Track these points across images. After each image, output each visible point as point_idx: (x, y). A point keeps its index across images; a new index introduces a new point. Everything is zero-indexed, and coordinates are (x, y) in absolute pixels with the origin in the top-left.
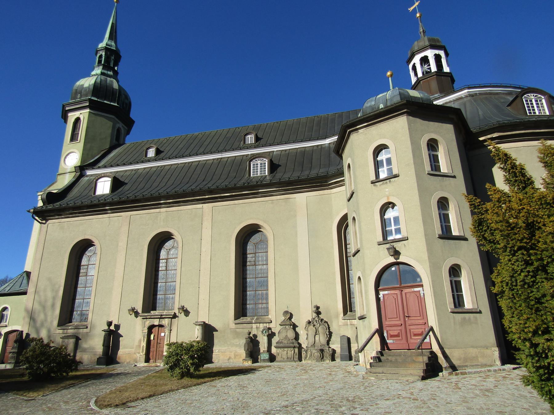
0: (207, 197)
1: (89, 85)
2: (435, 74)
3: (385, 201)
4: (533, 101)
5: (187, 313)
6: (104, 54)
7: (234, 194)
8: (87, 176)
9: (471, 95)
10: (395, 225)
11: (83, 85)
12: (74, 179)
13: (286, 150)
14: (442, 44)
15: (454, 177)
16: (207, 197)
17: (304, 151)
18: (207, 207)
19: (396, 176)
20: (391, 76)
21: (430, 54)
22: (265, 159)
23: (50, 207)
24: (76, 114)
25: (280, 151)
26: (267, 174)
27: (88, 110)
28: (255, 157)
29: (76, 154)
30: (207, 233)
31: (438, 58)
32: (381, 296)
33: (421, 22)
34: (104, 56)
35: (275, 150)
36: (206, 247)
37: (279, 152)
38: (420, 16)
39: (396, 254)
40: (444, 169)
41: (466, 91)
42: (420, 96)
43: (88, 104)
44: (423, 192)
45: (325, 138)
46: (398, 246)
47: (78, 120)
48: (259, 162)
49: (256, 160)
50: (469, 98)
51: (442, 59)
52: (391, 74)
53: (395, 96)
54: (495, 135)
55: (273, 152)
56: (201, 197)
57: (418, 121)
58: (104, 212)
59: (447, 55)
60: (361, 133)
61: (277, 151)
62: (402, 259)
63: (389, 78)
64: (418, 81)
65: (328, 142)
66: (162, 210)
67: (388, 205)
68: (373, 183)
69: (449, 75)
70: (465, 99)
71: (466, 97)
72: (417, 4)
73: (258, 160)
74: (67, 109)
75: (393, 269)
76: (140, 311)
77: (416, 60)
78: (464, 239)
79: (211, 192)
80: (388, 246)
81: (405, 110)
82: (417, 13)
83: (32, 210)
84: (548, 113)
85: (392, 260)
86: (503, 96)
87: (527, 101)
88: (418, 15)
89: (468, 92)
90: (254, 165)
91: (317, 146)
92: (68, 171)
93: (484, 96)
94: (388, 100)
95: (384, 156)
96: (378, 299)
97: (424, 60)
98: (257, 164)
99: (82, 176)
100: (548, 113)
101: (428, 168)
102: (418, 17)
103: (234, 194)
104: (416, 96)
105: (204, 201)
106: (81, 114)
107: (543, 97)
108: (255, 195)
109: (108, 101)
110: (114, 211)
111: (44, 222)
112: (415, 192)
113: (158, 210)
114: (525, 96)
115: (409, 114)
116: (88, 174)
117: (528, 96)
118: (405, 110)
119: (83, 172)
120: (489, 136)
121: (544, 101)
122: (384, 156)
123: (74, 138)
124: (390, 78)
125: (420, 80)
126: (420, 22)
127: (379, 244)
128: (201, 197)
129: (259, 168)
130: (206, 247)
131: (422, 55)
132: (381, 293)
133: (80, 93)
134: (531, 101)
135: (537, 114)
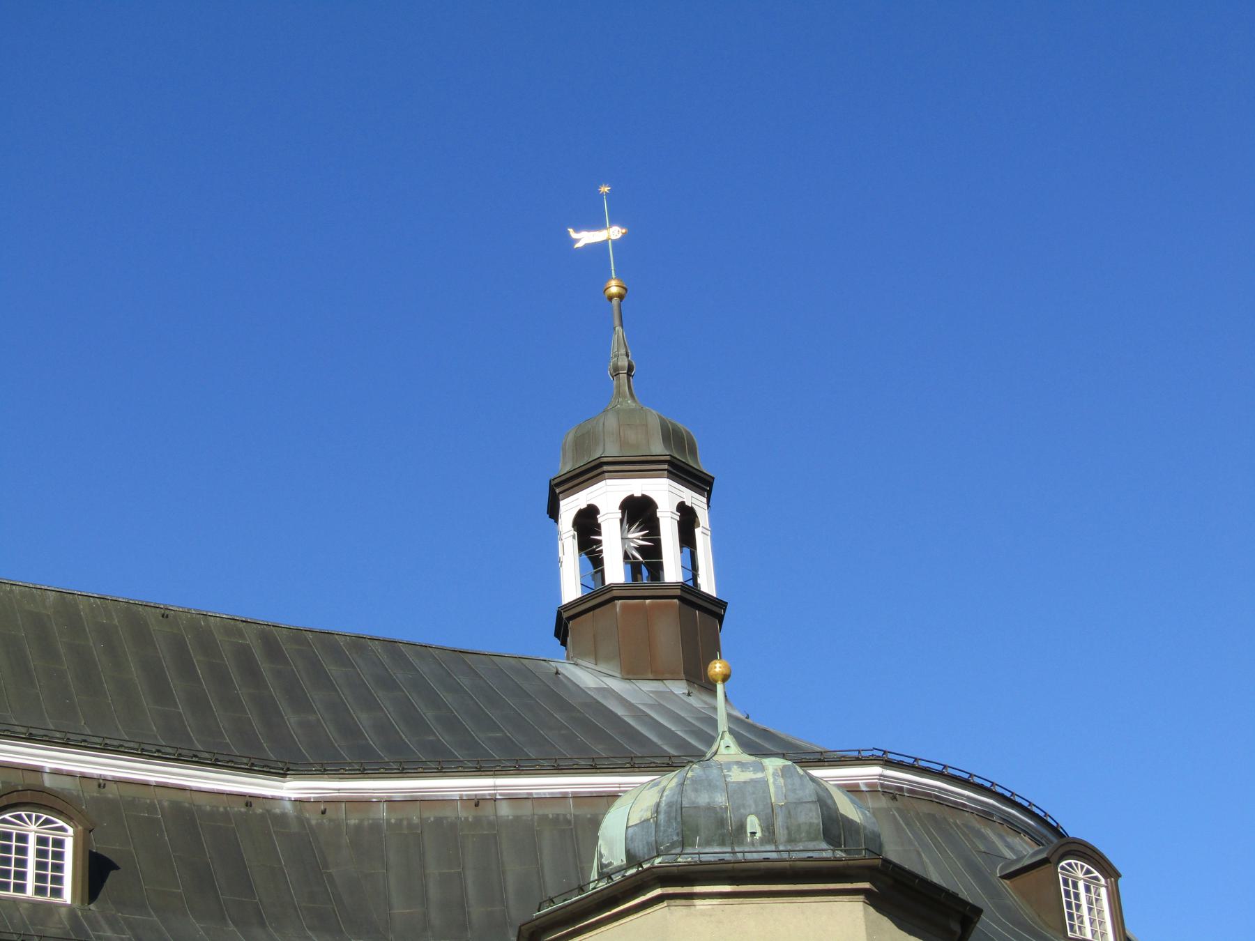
2: (678, 592)
4: (1081, 885)
9: (893, 793)
13: (102, 782)
14: (704, 465)
20: (725, 678)
22: (61, 823)
25: (70, 774)
26: (67, 897)
28: (14, 798)
33: (621, 325)
35: (48, 765)
37: (66, 784)
38: (621, 297)
41: (876, 770)
42: (858, 821)
45: (282, 772)
48: (33, 831)
49: (19, 818)
51: (698, 531)
52: (725, 671)
53: (799, 803)
55: (37, 770)
57: (886, 924)
60: (703, 913)
61: (57, 773)
63: (717, 682)
65: (294, 795)
69: (714, 609)
71: (873, 790)
72: (615, 233)
73: (29, 817)
81: (866, 885)
82: (610, 278)
86: (976, 823)
87: (1066, 882)
88: (614, 289)
89: (881, 776)
91: (249, 800)
93: (925, 808)
94: (777, 810)
98: (22, 838)
102: (610, 298)
104: (851, 817)
107: (1103, 881)
114: (1063, 863)
115: (874, 900)
117: (1070, 865)
118: (866, 885)
121: (1103, 891)
125: (615, 593)
126: (617, 322)
129: (31, 858)
134: (1075, 885)
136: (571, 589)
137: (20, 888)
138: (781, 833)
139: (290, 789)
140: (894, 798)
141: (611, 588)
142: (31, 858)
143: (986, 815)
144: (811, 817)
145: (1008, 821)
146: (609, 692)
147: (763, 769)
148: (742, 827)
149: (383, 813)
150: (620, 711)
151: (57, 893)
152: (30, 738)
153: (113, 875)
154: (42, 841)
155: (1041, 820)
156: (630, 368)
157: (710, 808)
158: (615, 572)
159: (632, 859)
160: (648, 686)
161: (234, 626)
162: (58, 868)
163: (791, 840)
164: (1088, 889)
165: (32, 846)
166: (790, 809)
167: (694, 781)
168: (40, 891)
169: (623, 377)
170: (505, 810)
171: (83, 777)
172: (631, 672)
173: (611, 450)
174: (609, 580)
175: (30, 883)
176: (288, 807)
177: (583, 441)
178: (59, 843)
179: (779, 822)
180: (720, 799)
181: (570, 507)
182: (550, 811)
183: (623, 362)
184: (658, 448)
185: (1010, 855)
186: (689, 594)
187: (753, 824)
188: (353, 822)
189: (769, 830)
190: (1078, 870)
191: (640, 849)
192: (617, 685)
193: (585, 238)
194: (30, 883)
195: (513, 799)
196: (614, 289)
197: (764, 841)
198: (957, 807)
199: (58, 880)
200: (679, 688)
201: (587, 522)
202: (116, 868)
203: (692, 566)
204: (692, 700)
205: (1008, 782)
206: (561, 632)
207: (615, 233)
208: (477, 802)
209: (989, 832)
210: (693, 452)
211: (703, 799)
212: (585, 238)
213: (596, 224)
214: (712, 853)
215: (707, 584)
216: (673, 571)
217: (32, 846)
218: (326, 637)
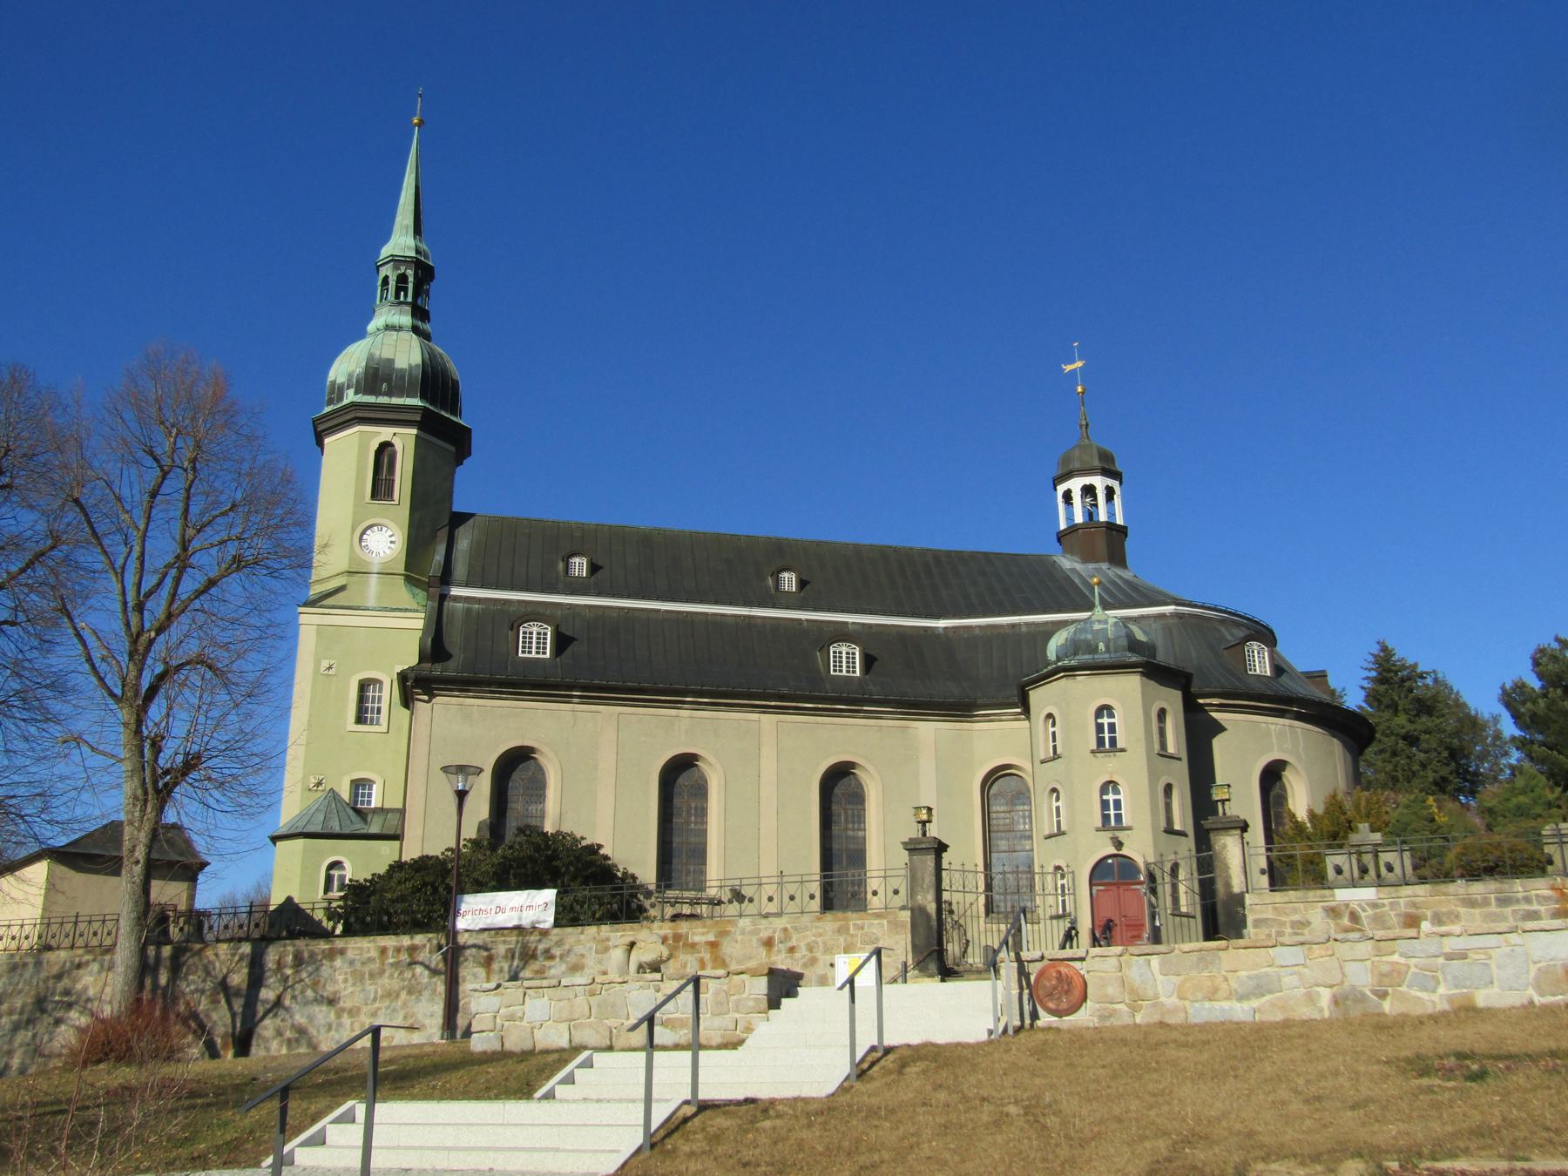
0: (773, 703)
1: (410, 365)
3: (1108, 778)
4: (1256, 652)
5: (738, 896)
6: (410, 273)
7: (820, 706)
8: (457, 599)
10: (1115, 810)
11: (391, 362)
12: (436, 604)
13: (870, 626)
14: (1119, 467)
15: (1180, 759)
16: (773, 703)
17: (902, 634)
18: (768, 720)
19: (1123, 750)
21: (1099, 482)
23: (437, 670)
24: (385, 433)
26: (858, 674)
27: (414, 431)
29: (386, 533)
30: (769, 766)
31: (1110, 492)
32: (1094, 891)
34: (411, 279)
35: (850, 620)
36: (768, 791)
37: (857, 627)
38: (1083, 393)
39: (1119, 844)
40: (1171, 749)
41: (1174, 607)
43: (419, 419)
44: (1153, 776)
46: (1121, 835)
47: (385, 447)
48: (844, 649)
50: (1176, 620)
53: (1120, 637)
54: (1215, 701)
55: (847, 623)
56: (763, 703)
58: (567, 699)
59: (1121, 484)
61: (853, 623)
62: (1124, 851)
64: (1073, 529)
66: (682, 712)
67: (1109, 786)
68: (1093, 752)
69: (1122, 531)
70: (1170, 621)
72: (1079, 364)
74: (360, 414)
75: (1110, 861)
76: (652, 887)
77: (1076, 485)
78: (1182, 834)
79: (782, 698)
80: (1110, 834)
83: (412, 675)
84: (1269, 674)
85: (1113, 851)
88: (1080, 389)
90: (835, 652)
92: (375, 570)
95: (1105, 718)
96: (1091, 894)
97: (1089, 491)
99: (443, 598)
100: (1269, 674)
101: (1157, 747)
103: (820, 706)
105: (765, 709)
108: (853, 713)
109: (446, 411)
110: (585, 700)
111: (426, 698)
112: (1145, 774)
113: (673, 712)
115: (1143, 674)
116: (452, 593)
119: (445, 587)
120: (1208, 701)
121: (1266, 653)
122: (1105, 718)
123: (381, 488)
124: (1096, 587)
127: (1098, 830)
128: (763, 703)
129: (844, 660)
130: (768, 791)
131: (1087, 480)
132: (1095, 888)
133: (388, 379)
135: (1258, 672)
136: (1063, 526)
137: (841, 671)
138: (1112, 649)
139: (942, 624)
140: (1181, 618)
141: (1076, 525)
142: (844, 660)
143: (1223, 621)
144: (1124, 642)
145: (1234, 621)
146: (1074, 570)
147: (1106, 622)
148: (1097, 647)
149: (977, 631)
150: (1077, 581)
151: (854, 672)
152: (843, 611)
153: (876, 663)
154: (848, 653)
155: (1248, 619)
156: (1087, 425)
157: (1085, 640)
158: (1079, 518)
159: (1059, 659)
160: (1091, 566)
161: (924, 552)
162: (854, 663)
163: (1116, 652)
164: (1259, 653)
165: (844, 655)
166: (1116, 639)
167: (1080, 629)
168: (848, 672)
169: (1084, 429)
170: (1024, 629)
171: (863, 624)
172: (1086, 559)
173: (1076, 465)
174: (1076, 522)
175: (844, 669)
176: (941, 631)
177: (1066, 459)
178: (854, 654)
179: (1111, 645)
180: (1089, 637)
181: (1061, 489)
182: (1042, 629)
183: (1084, 423)
184: (1096, 463)
185: (1229, 638)
186: (1111, 526)
187: (1101, 646)
188: (966, 636)
189: (1107, 647)
190: (1255, 645)
191: (1061, 655)
192: (1078, 566)
193: (1069, 368)
194: (844, 669)
195: (1027, 624)
196: (1080, 389)
197: (1105, 652)
198: (1210, 619)
199: (854, 667)
200: (1104, 566)
201: (1068, 496)
202: (876, 659)
203: (1111, 514)
204: (1108, 571)
205: (1232, 607)
206: (1059, 540)
207: (1079, 364)
208: (1013, 626)
209: (1223, 629)
210: (1113, 460)
211: (1083, 637)
212: (1069, 368)
213: (1073, 362)
214: (1085, 658)
215: (1119, 521)
216: (1103, 516)
217: (844, 655)
218: (960, 555)
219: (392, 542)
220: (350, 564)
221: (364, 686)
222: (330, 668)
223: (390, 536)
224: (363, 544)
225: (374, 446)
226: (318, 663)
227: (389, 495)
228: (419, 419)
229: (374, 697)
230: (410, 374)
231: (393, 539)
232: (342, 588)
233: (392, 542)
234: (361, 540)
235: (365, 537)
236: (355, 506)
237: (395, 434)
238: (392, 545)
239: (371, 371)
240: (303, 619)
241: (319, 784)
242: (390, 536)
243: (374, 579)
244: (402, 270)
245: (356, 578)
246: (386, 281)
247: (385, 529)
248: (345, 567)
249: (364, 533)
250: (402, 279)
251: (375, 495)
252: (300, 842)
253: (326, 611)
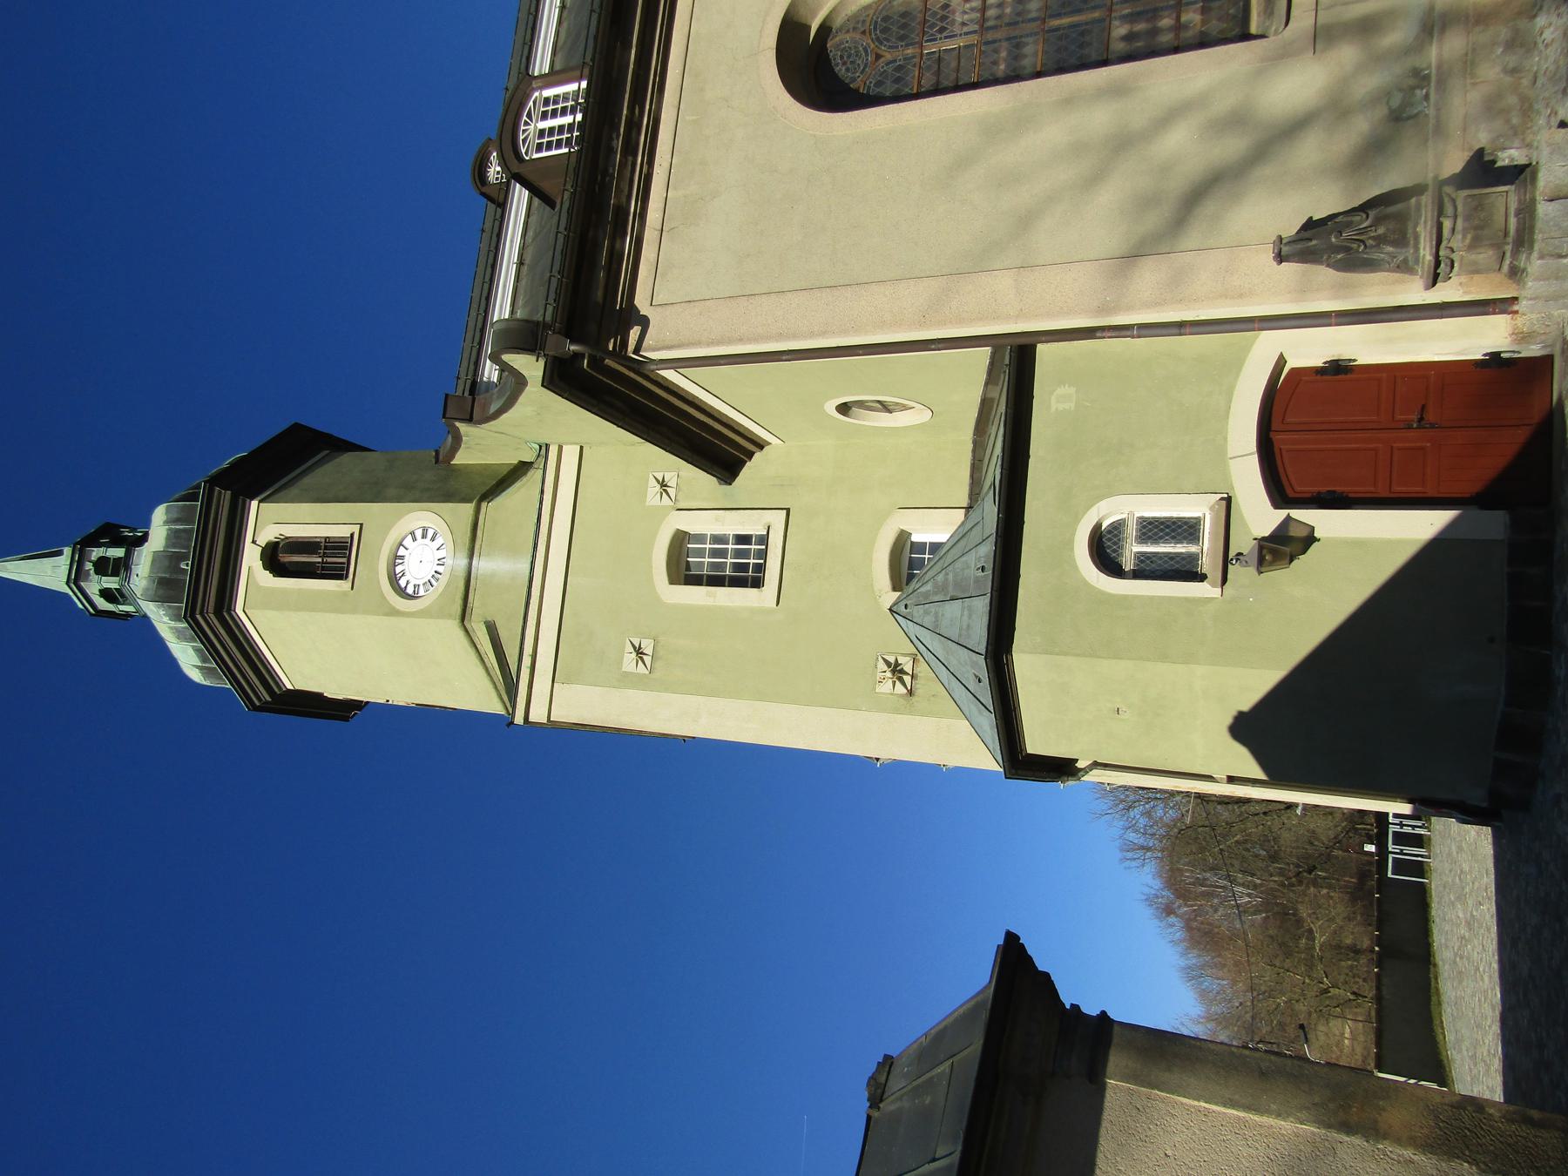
6: (96, 553)
24: (251, 557)
43: (228, 495)
106: (254, 542)
111: (634, 333)
219: (433, 539)
220: (450, 616)
221: (683, 572)
222: (639, 652)
223: (414, 539)
224: (410, 590)
225: (266, 578)
226: (627, 680)
227: (341, 547)
228: (228, 495)
229: (715, 553)
230: (177, 521)
231: (419, 533)
232: (492, 629)
233: (424, 536)
234: (402, 592)
235: (402, 583)
236: (354, 611)
237: (254, 542)
238: (439, 541)
239: (161, 592)
240: (538, 715)
241: (897, 670)
242: (414, 539)
243: (482, 565)
244: (89, 566)
245: (475, 601)
246: (107, 594)
247: (402, 552)
248: (453, 626)
249: (394, 579)
250: (102, 567)
251: (338, 573)
252: (1025, 664)
253: (527, 661)
